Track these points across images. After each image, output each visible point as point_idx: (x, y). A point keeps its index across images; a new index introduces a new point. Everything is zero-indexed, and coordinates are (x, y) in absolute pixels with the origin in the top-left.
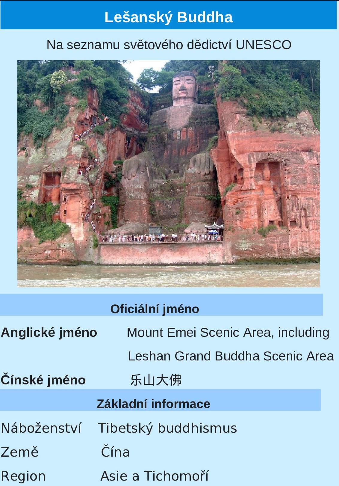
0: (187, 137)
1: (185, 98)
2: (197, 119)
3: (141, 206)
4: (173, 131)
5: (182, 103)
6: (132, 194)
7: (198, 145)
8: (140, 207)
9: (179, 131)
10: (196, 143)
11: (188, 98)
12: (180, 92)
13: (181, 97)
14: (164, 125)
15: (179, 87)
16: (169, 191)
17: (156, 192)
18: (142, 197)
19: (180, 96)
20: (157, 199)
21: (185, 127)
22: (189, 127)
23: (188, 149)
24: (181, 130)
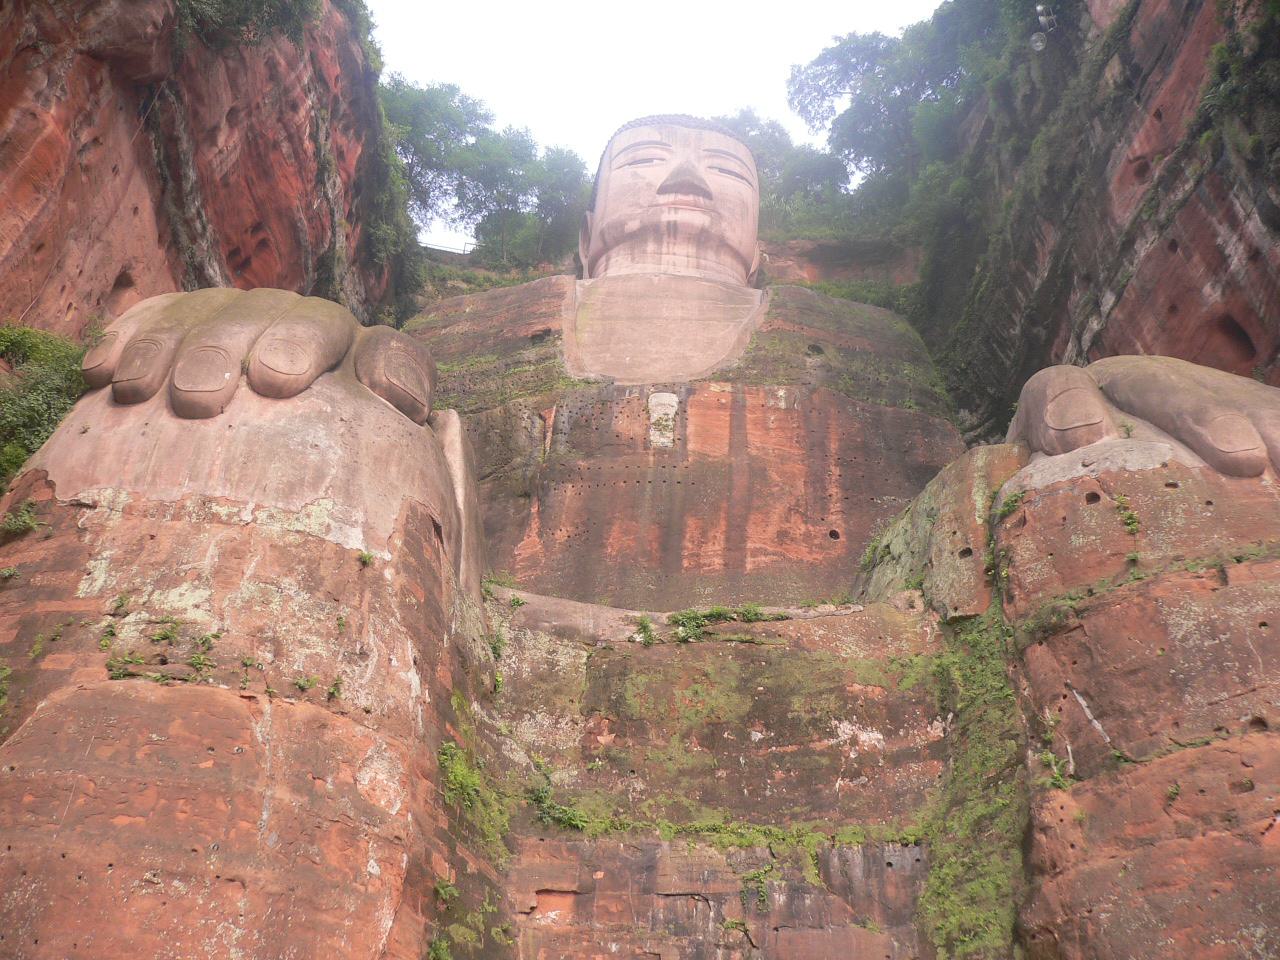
0: (738, 442)
1: (701, 239)
2: (816, 349)
3: (323, 820)
4: (607, 397)
5: (678, 259)
6: (186, 601)
7: (836, 520)
8: (299, 832)
9: (670, 401)
10: (823, 501)
11: (723, 245)
13: (673, 229)
14: (531, 354)
15: (658, 174)
16: (711, 735)
17: (527, 731)
18: (358, 692)
19: (667, 217)
20: (546, 816)
21: (722, 376)
22: (758, 381)
23: (759, 536)
24: (688, 392)
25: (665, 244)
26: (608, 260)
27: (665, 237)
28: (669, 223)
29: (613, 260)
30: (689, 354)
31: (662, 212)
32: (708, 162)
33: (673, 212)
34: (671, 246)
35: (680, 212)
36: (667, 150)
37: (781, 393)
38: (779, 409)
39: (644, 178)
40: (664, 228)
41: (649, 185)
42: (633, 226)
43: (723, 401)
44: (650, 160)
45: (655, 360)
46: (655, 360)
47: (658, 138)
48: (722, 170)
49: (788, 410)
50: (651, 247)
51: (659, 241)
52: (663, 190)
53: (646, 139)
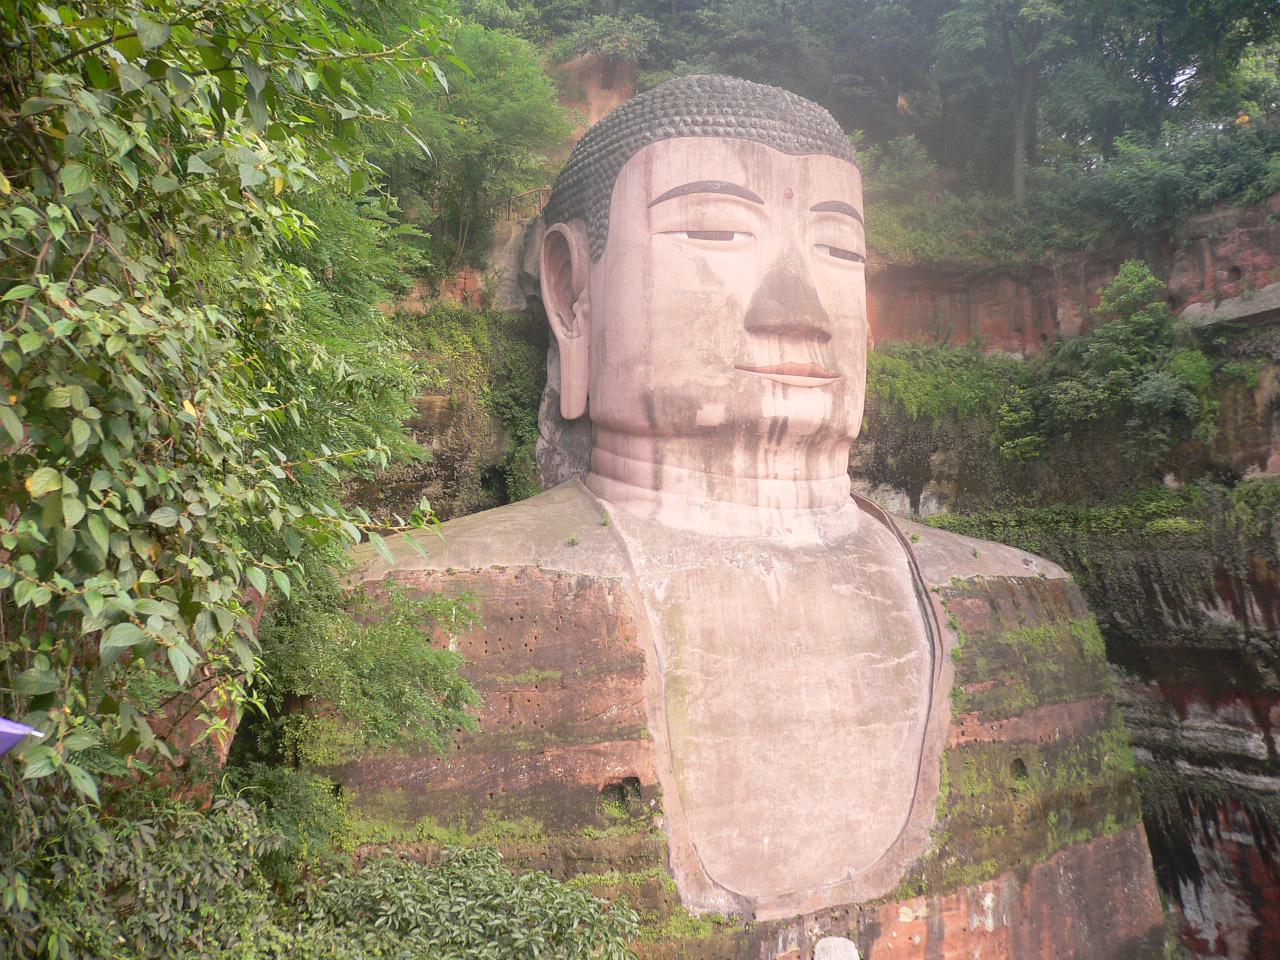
12: (765, 352)
13: (779, 430)
15: (740, 273)
19: (773, 406)
25: (761, 455)
26: (658, 461)
27: (763, 444)
28: (775, 421)
29: (670, 470)
30: (854, 816)
31: (762, 389)
32: (814, 234)
33: (779, 391)
34: (770, 456)
35: (791, 392)
36: (760, 213)
37: (988, 901)
38: (983, 933)
39: (721, 284)
40: (765, 428)
41: (732, 303)
42: (712, 414)
43: (917, 940)
44: (726, 235)
45: (806, 840)
46: (806, 840)
47: (738, 178)
48: (835, 252)
49: (997, 931)
50: (739, 459)
51: (752, 447)
52: (757, 328)
53: (721, 177)
